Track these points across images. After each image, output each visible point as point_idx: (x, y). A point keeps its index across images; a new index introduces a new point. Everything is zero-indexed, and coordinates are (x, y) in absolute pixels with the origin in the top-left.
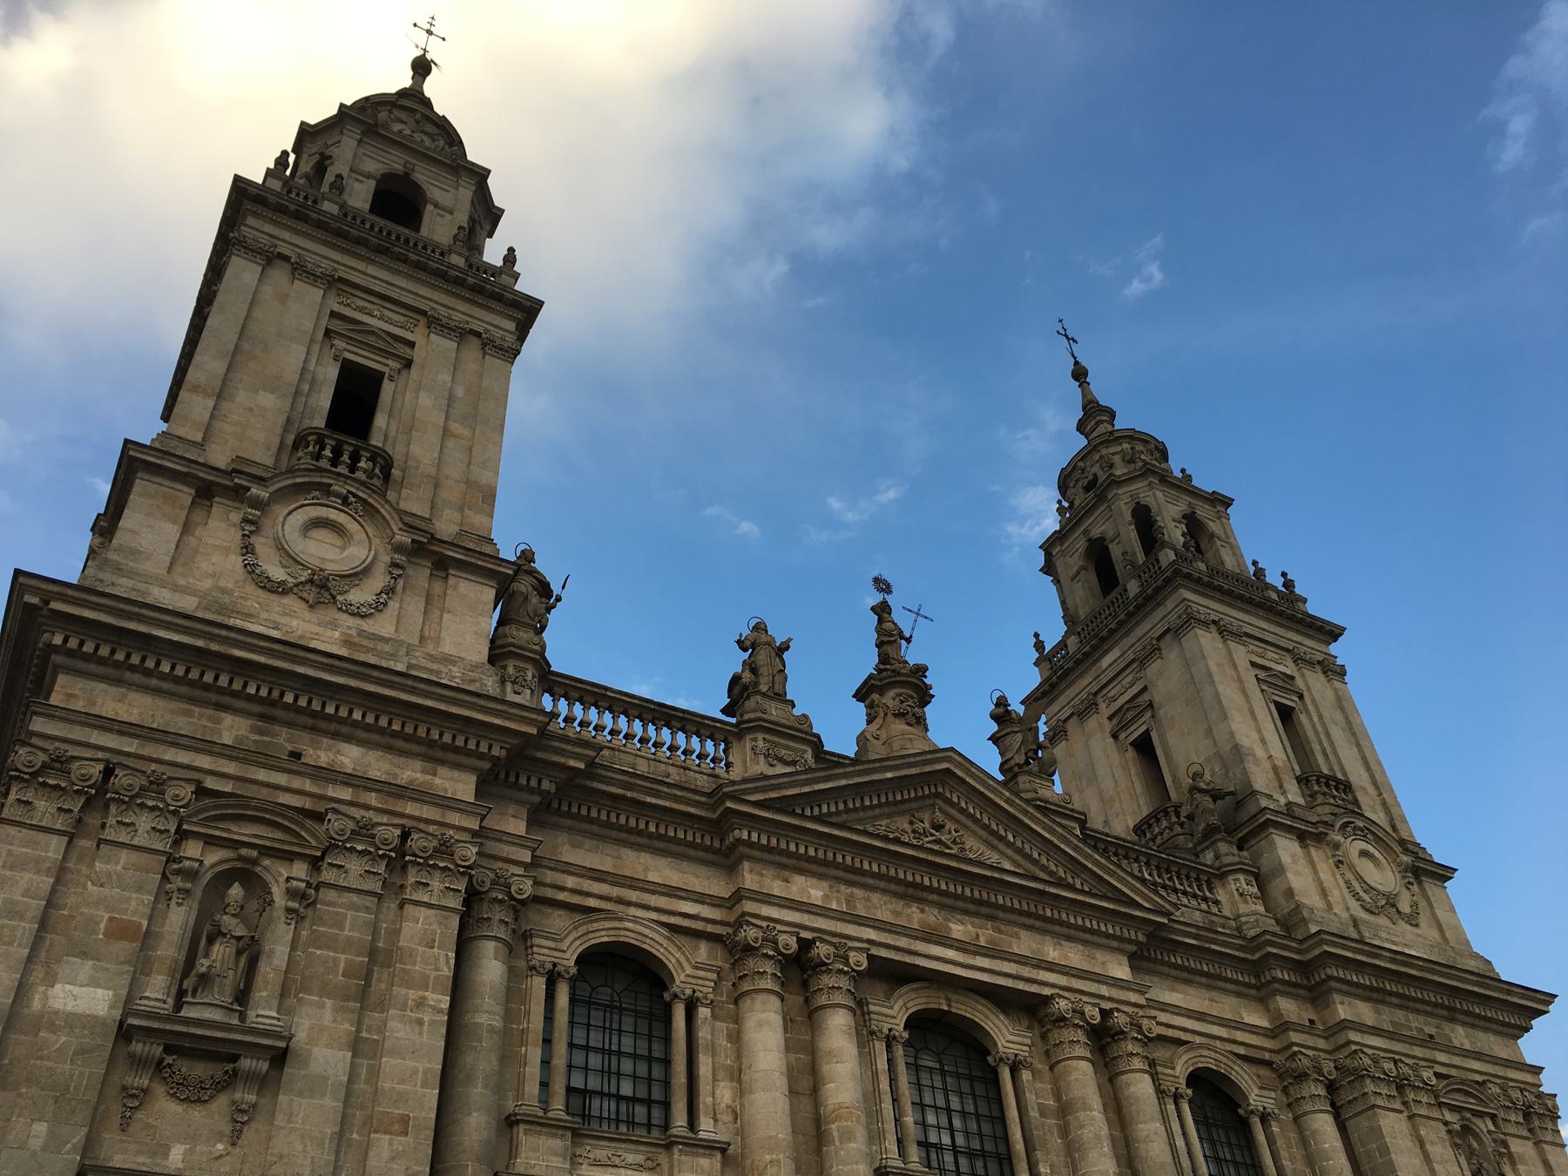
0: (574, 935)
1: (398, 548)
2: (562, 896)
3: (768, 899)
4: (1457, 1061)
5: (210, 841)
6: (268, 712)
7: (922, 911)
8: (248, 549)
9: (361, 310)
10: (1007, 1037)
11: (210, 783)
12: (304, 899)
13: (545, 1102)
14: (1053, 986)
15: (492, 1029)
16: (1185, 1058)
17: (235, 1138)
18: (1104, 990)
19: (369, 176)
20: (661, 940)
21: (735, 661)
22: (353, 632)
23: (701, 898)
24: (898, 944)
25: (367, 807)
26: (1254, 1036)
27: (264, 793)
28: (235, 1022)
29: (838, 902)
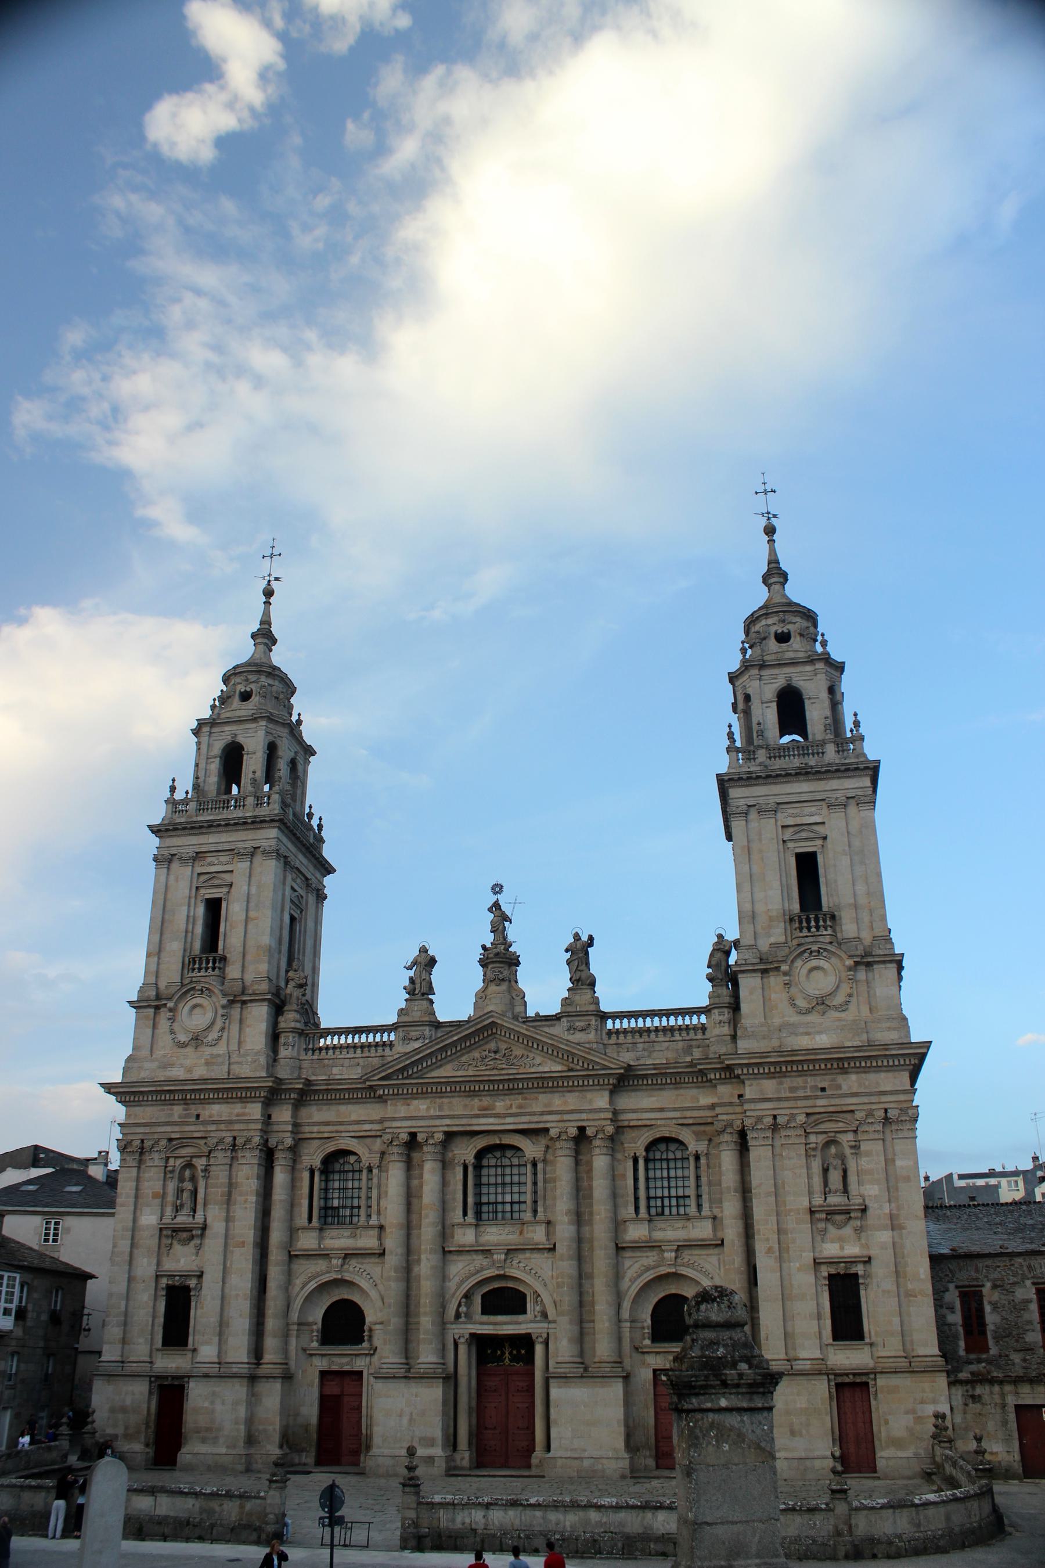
0: (319, 1151)
1: (223, 1007)
2: (314, 1135)
3: (394, 1119)
4: (833, 1102)
5: (176, 1157)
6: (185, 1101)
7: (481, 1100)
8: (172, 1032)
9: (212, 864)
11: (173, 1136)
13: (310, 1219)
14: (553, 1122)
15: (281, 1201)
16: (647, 1134)
17: (197, 1254)
18: (584, 1116)
19: (215, 758)
21: (405, 977)
22: (209, 1057)
23: (372, 1122)
24: (462, 1123)
25: (222, 1131)
26: (701, 1111)
27: (189, 1135)
29: (435, 1109)
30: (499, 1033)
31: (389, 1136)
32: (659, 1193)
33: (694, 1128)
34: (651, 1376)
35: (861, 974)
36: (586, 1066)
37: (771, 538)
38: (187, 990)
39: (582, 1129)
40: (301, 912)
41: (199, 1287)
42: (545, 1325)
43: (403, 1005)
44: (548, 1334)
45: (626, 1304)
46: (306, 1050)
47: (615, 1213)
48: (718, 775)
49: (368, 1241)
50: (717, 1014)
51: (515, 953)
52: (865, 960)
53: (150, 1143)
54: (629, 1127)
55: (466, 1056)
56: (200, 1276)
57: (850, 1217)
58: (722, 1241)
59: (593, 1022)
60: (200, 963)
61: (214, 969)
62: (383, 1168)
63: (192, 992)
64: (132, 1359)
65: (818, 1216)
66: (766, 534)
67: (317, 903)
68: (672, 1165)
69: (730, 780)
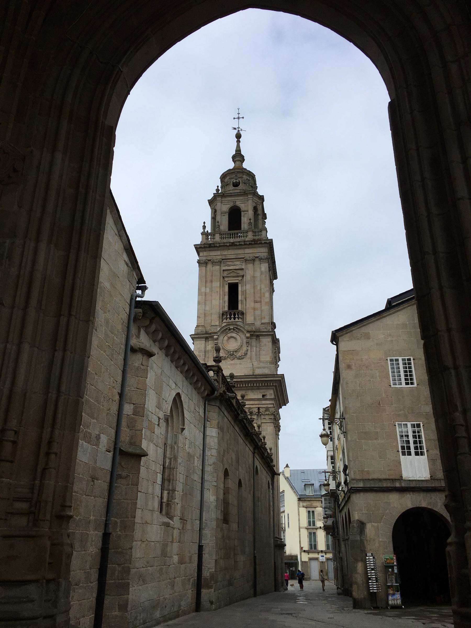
35: (254, 342)
37: (239, 140)
48: (194, 245)
52: (255, 334)
66: (236, 138)
69: (200, 248)
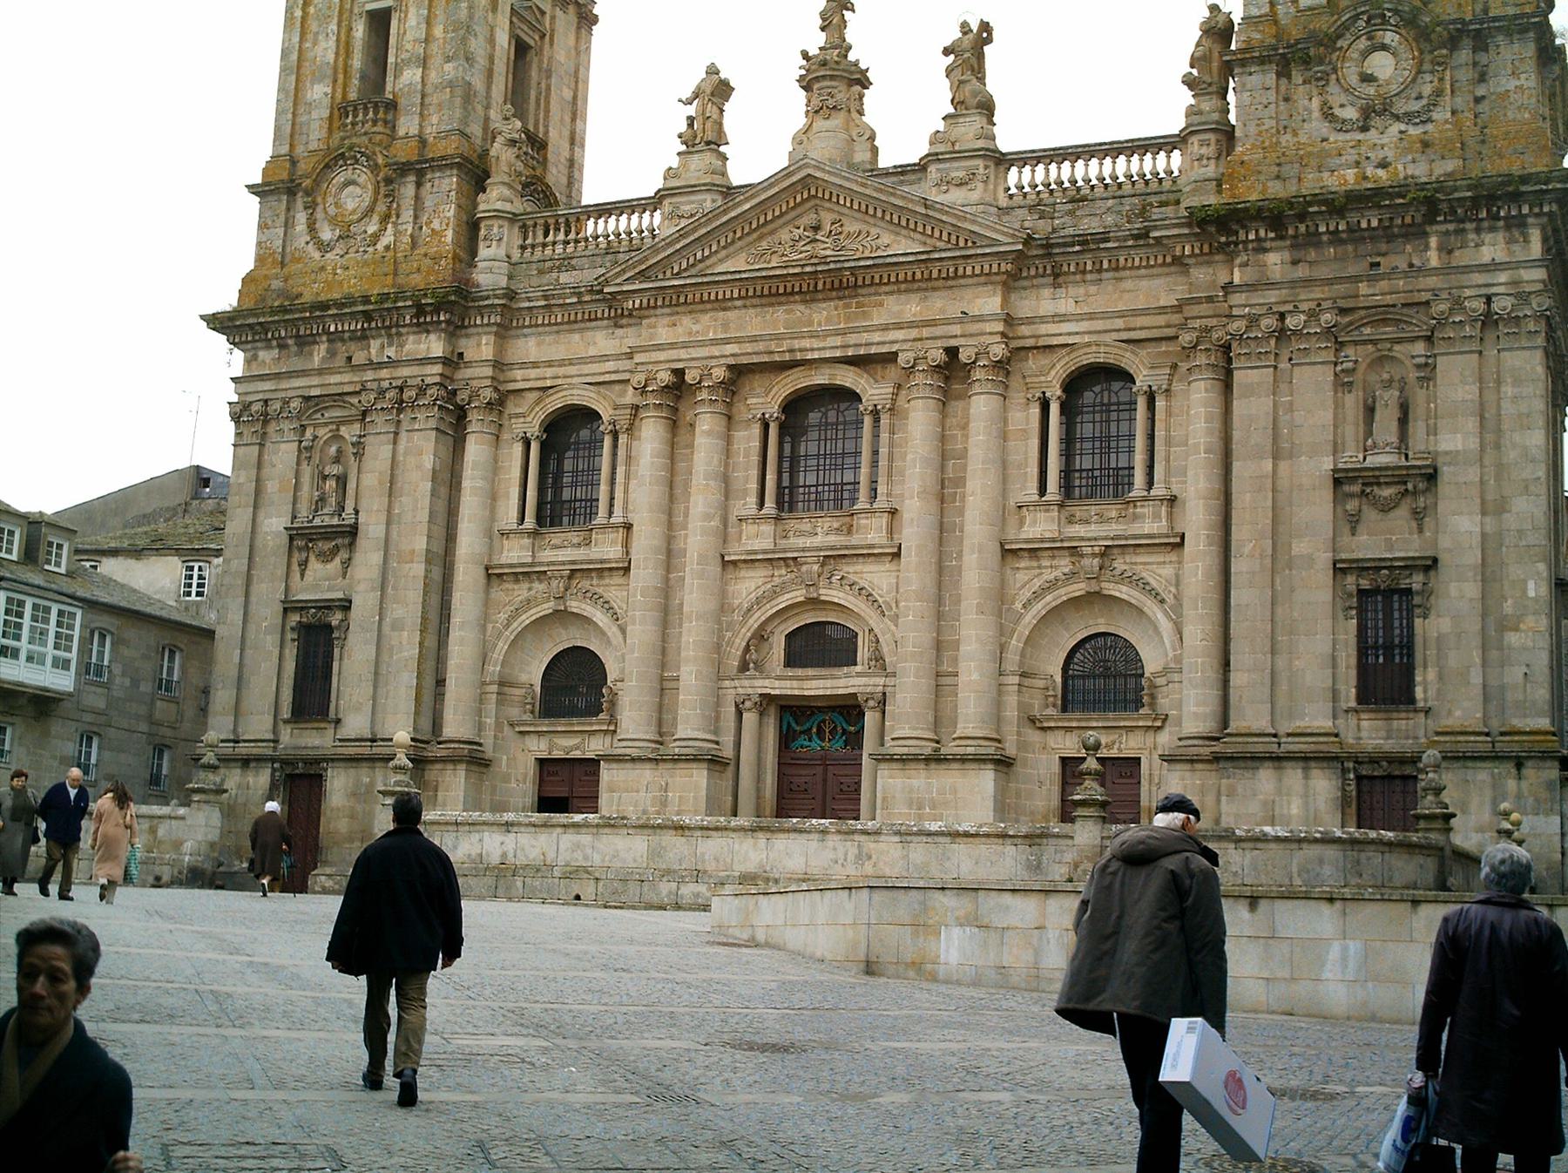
5: (315, 426)
7: (787, 312)
8: (312, 228)
10: (872, 390)
12: (359, 445)
16: (1067, 359)
18: (956, 329)
20: (592, 395)
28: (335, 521)
30: (820, 195)
31: (642, 377)
32: (1087, 465)
33: (1152, 349)
34: (1056, 767)
36: (962, 244)
38: (334, 160)
39: (952, 352)
40: (543, 36)
41: (345, 626)
42: (881, 681)
43: (675, 162)
44: (884, 694)
45: (1015, 643)
46: (523, 248)
47: (1004, 493)
49: (607, 548)
50: (1196, 143)
51: (856, 64)
53: (277, 406)
54: (1036, 348)
55: (769, 239)
56: (346, 605)
57: (1406, 490)
58: (1183, 537)
59: (981, 170)
60: (355, 116)
61: (375, 122)
62: (636, 434)
63: (341, 162)
64: (245, 738)
65: (1346, 488)
67: (579, 28)
68: (1114, 416)
